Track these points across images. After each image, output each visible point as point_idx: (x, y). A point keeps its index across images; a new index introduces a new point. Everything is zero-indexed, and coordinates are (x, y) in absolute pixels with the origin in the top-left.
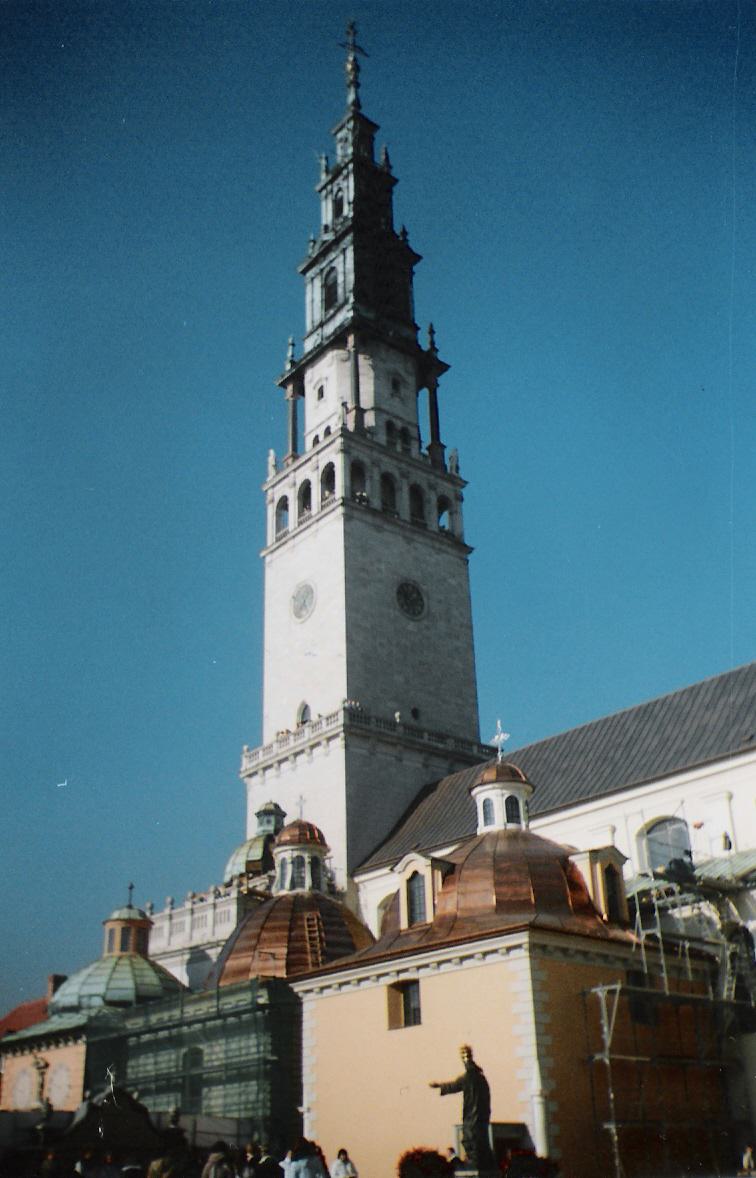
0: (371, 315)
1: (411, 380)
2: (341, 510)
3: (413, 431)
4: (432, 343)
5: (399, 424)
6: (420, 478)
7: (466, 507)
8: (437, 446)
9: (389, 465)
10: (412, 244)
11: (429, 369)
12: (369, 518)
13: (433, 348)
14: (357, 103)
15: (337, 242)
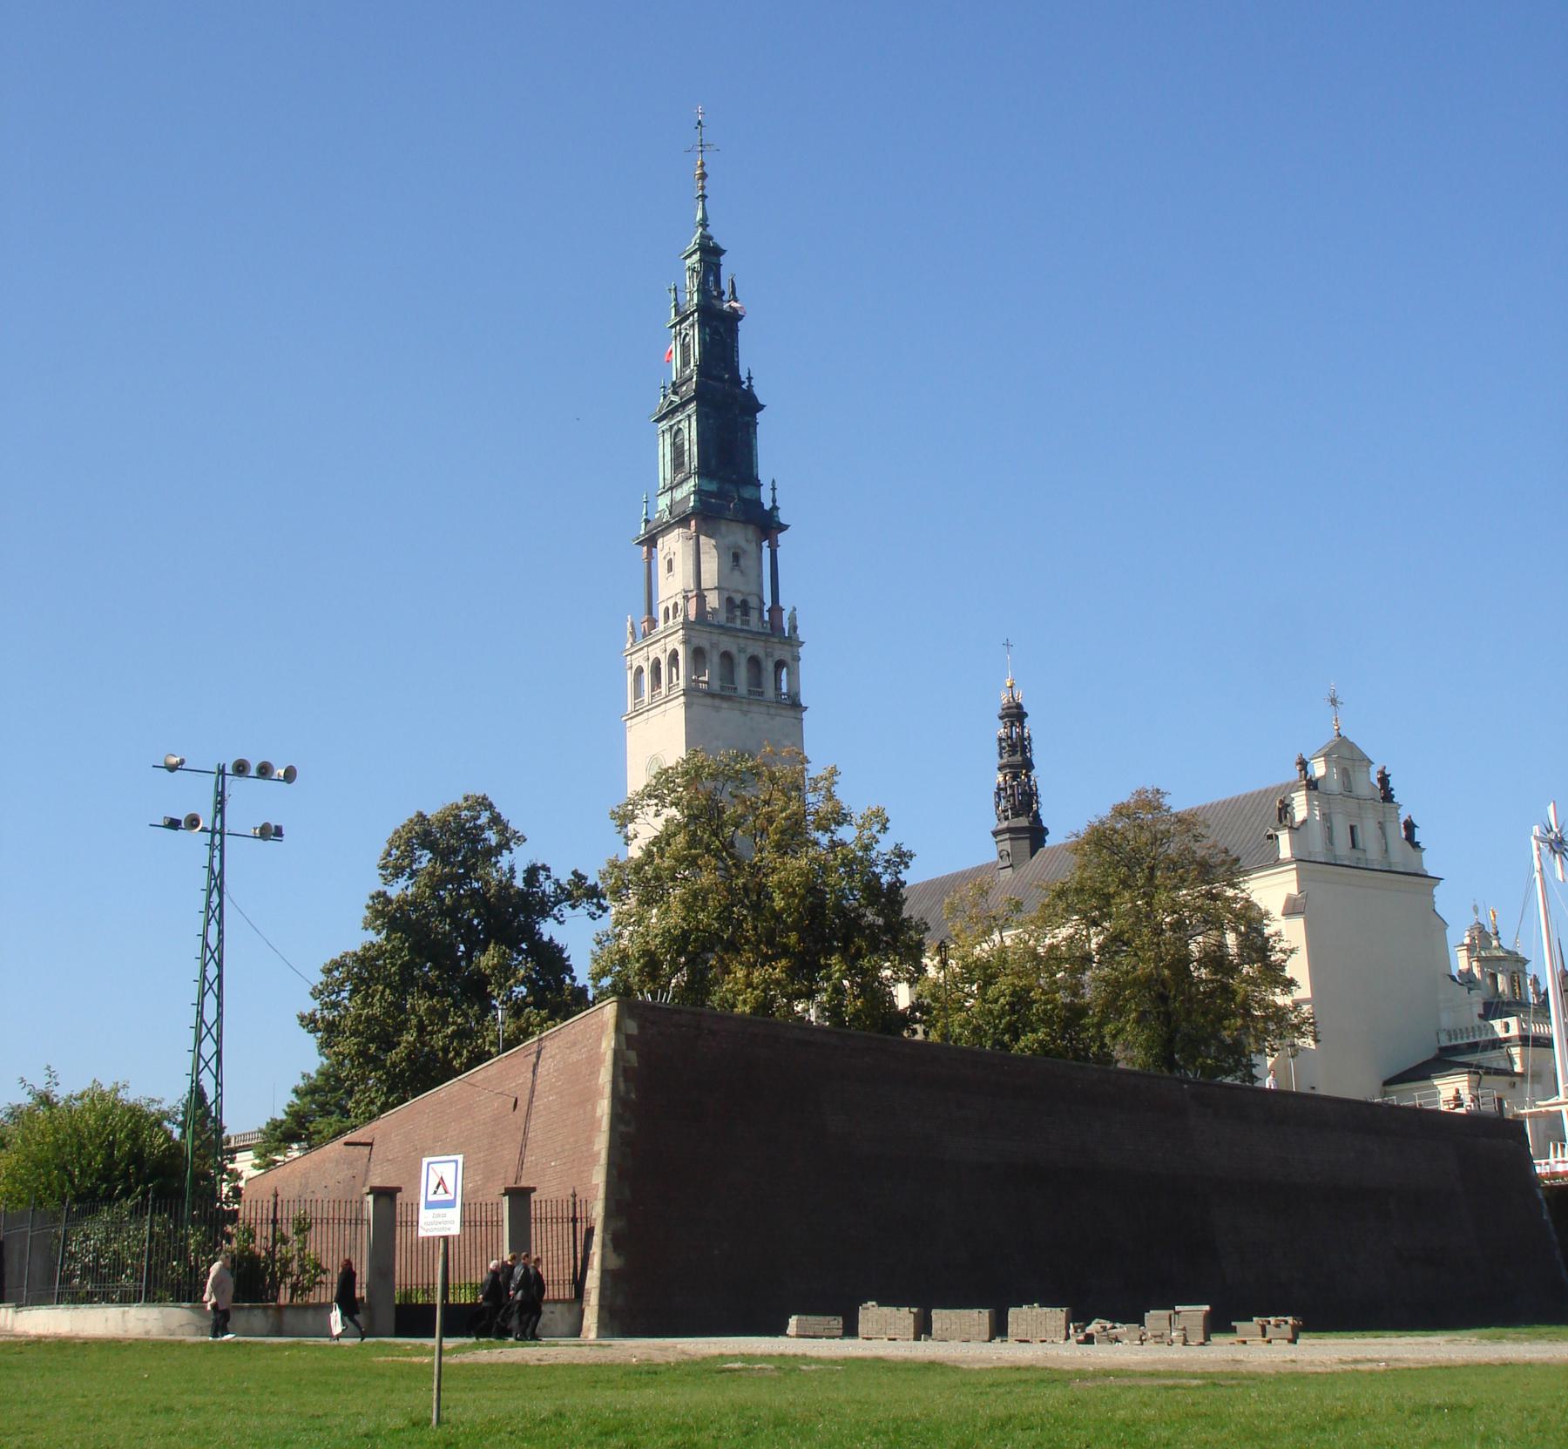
0: (712, 487)
1: (752, 548)
2: (682, 699)
3: (753, 602)
4: (774, 501)
5: (738, 598)
6: (756, 648)
7: (804, 667)
8: (776, 609)
9: (727, 643)
10: (757, 391)
11: (767, 525)
12: (709, 701)
13: (775, 508)
14: (704, 223)
15: (684, 405)
